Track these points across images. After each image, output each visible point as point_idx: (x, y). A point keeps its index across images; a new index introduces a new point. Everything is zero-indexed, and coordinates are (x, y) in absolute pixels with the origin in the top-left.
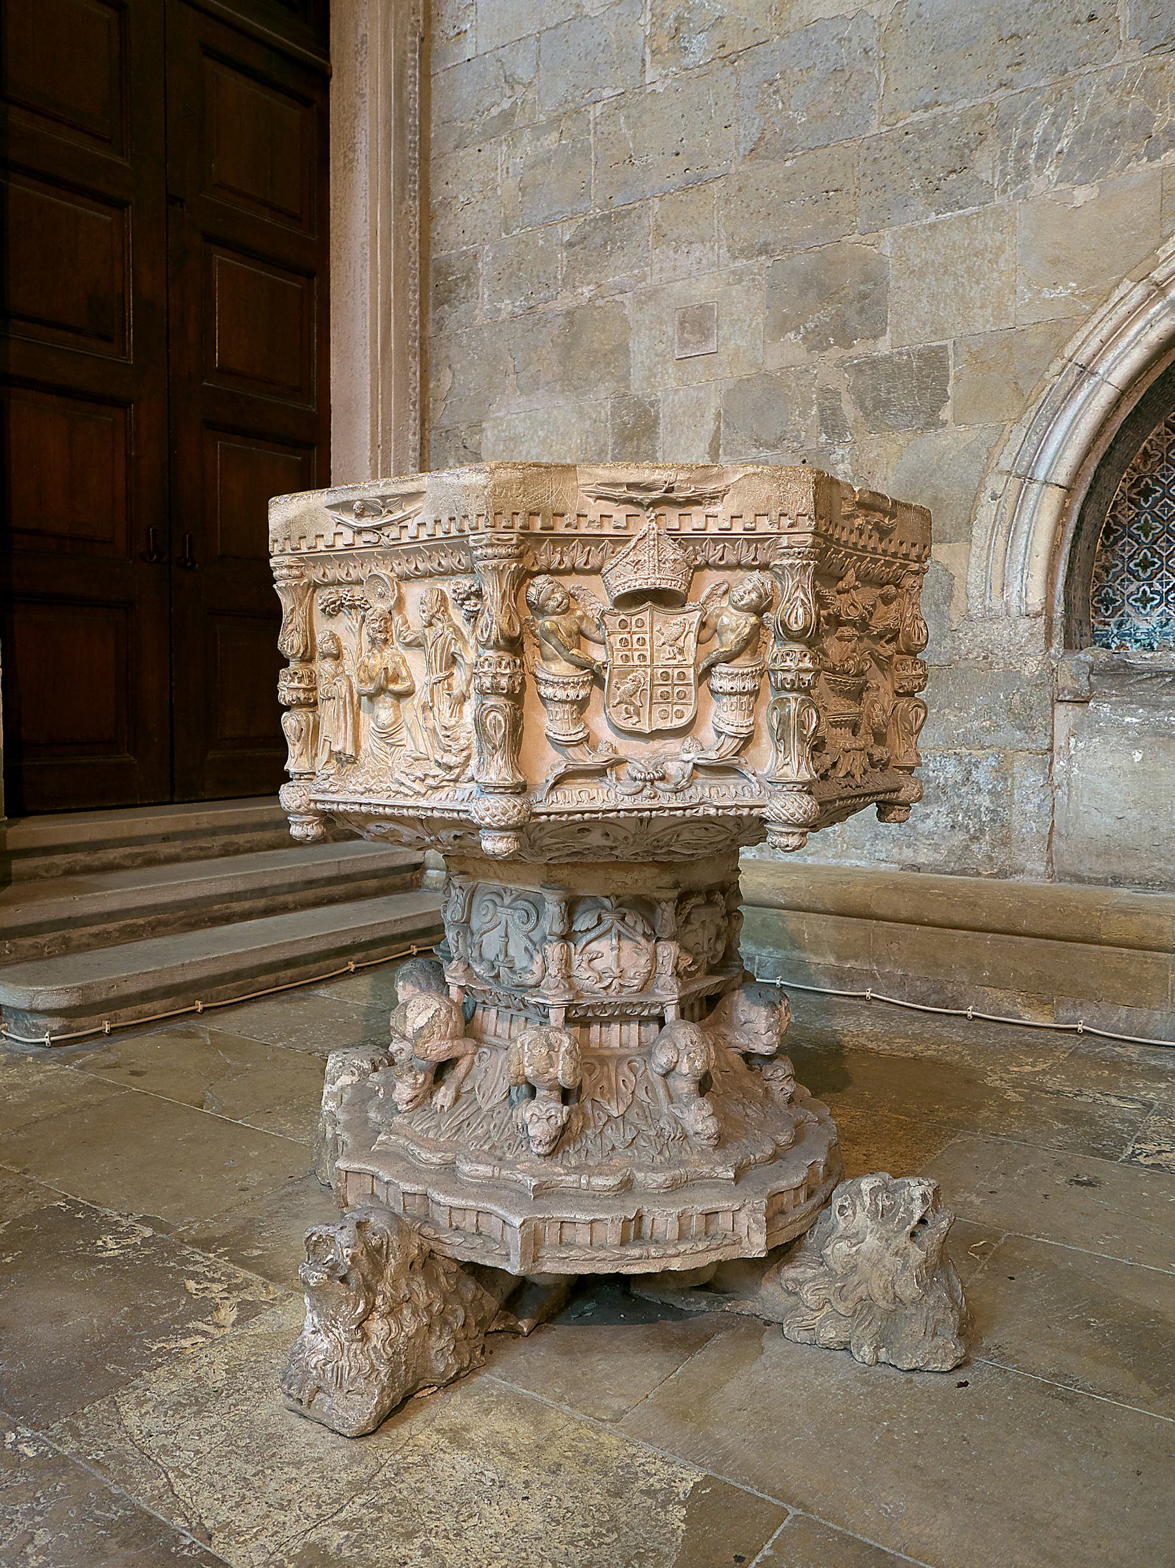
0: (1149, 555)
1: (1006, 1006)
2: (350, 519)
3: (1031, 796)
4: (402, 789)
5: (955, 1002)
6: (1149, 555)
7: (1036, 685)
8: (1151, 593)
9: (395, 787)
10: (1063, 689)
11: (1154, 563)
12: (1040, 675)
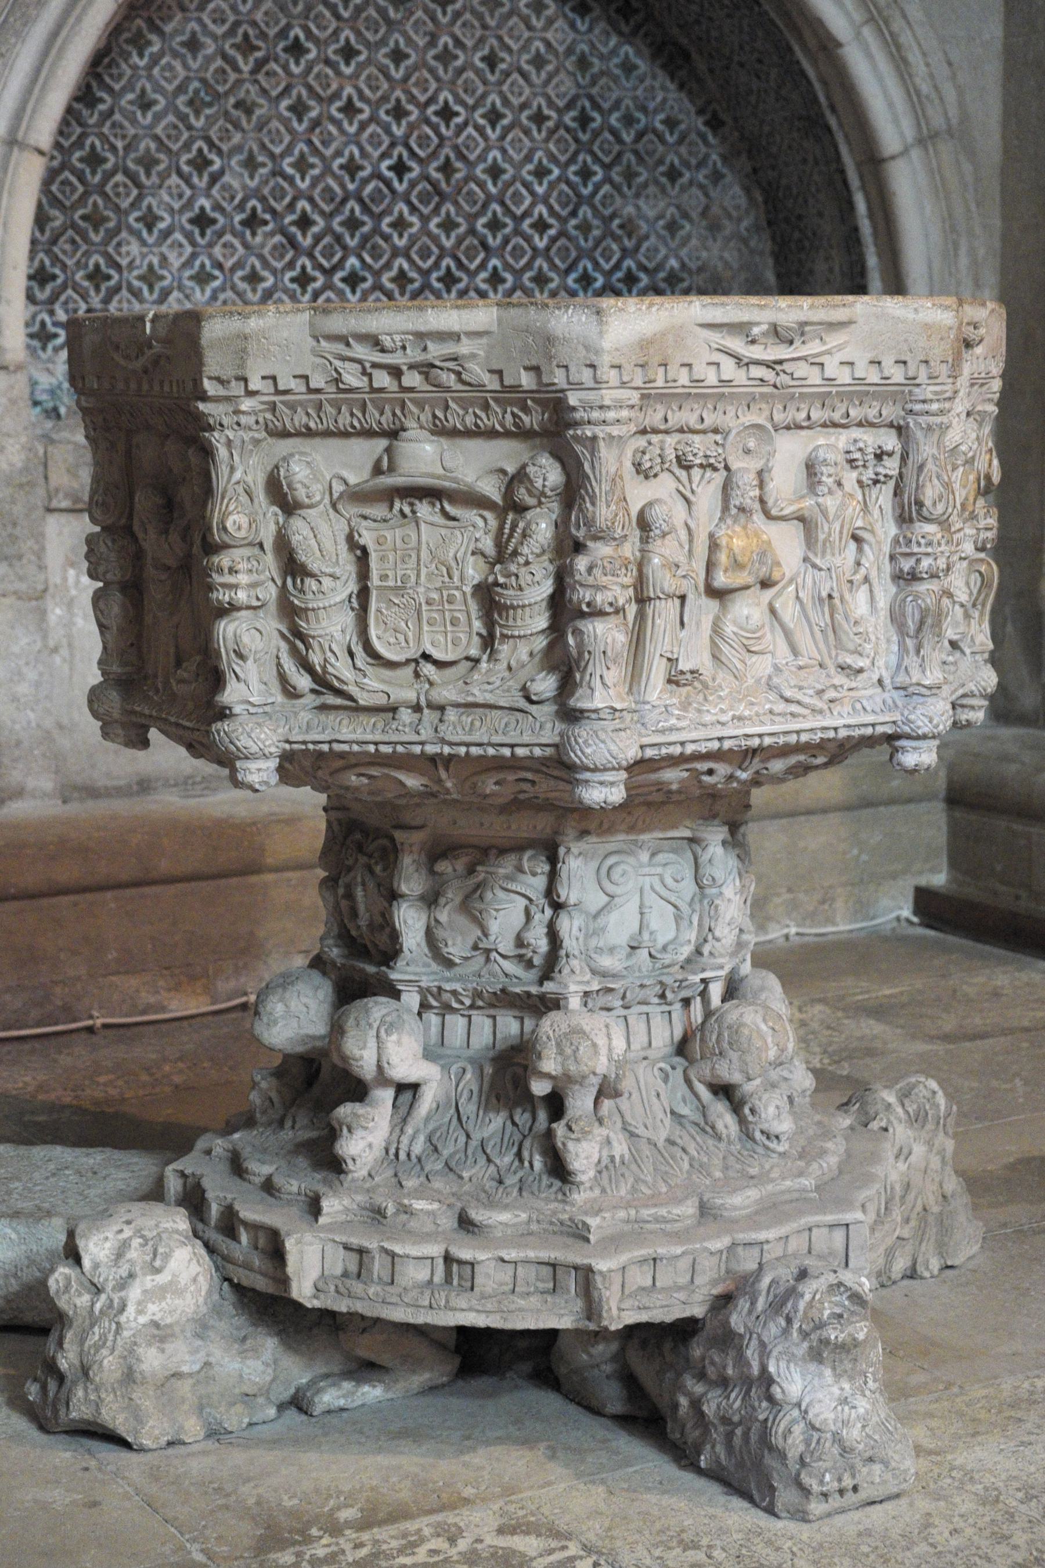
0: (47, 262)
1: (147, 998)
2: (737, 344)
3: (25, 670)
4: (794, 708)
5: (68, 1013)
6: (47, 262)
7: (21, 486)
8: (55, 324)
9: (781, 707)
10: (57, 490)
11: (54, 277)
12: (26, 469)
